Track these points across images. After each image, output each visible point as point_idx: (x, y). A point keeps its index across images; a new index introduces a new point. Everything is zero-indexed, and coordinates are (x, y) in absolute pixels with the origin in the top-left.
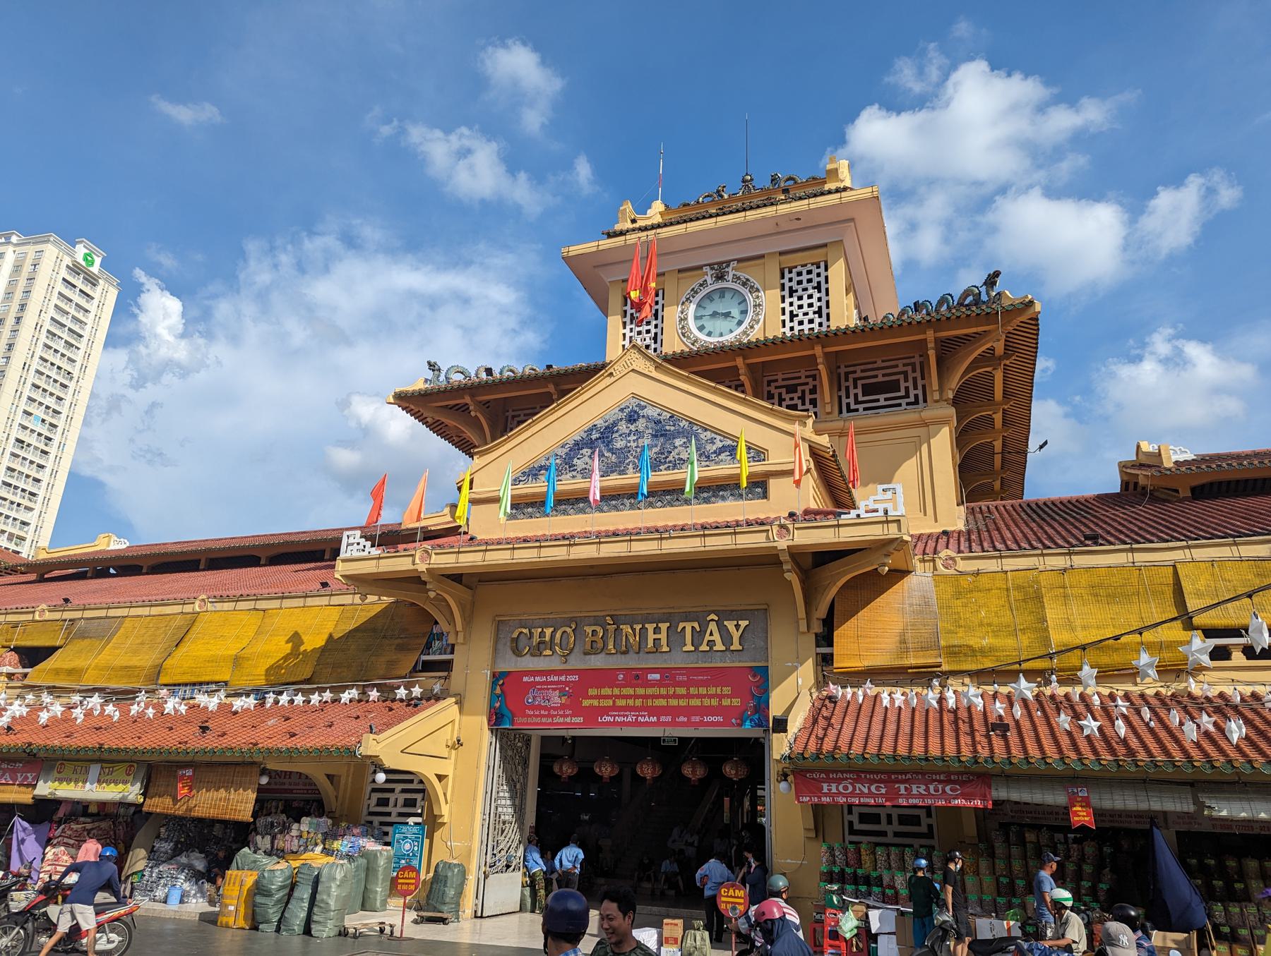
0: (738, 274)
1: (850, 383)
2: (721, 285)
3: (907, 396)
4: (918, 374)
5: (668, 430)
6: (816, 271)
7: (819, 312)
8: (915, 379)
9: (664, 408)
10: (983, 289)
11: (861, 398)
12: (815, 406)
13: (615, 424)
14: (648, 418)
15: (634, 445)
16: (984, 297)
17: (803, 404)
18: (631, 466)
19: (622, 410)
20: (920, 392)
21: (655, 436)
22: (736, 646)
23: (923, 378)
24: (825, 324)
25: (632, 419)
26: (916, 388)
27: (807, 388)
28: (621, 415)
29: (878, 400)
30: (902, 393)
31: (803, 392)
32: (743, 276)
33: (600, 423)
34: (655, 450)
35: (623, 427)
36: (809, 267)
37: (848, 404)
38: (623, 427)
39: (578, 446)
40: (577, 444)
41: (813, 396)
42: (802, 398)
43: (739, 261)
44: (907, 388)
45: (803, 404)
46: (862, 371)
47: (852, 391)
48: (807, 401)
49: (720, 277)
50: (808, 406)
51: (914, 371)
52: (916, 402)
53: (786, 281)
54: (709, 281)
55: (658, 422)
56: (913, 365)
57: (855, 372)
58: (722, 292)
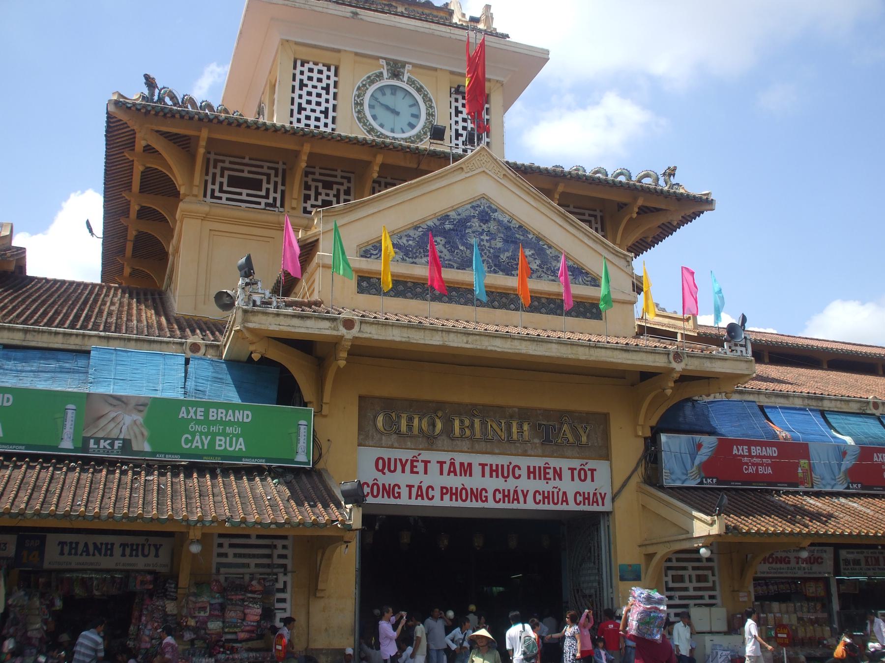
0: (414, 78)
5: (515, 235)
9: (512, 217)
13: (468, 219)
14: (500, 223)
15: (487, 244)
16: (661, 182)
19: (473, 207)
21: (506, 241)
24: (331, 126)
28: (472, 212)
33: (453, 214)
34: (507, 254)
38: (475, 223)
39: (432, 231)
40: (430, 229)
43: (415, 66)
49: (396, 75)
54: (385, 75)
55: (508, 228)
58: (394, 89)
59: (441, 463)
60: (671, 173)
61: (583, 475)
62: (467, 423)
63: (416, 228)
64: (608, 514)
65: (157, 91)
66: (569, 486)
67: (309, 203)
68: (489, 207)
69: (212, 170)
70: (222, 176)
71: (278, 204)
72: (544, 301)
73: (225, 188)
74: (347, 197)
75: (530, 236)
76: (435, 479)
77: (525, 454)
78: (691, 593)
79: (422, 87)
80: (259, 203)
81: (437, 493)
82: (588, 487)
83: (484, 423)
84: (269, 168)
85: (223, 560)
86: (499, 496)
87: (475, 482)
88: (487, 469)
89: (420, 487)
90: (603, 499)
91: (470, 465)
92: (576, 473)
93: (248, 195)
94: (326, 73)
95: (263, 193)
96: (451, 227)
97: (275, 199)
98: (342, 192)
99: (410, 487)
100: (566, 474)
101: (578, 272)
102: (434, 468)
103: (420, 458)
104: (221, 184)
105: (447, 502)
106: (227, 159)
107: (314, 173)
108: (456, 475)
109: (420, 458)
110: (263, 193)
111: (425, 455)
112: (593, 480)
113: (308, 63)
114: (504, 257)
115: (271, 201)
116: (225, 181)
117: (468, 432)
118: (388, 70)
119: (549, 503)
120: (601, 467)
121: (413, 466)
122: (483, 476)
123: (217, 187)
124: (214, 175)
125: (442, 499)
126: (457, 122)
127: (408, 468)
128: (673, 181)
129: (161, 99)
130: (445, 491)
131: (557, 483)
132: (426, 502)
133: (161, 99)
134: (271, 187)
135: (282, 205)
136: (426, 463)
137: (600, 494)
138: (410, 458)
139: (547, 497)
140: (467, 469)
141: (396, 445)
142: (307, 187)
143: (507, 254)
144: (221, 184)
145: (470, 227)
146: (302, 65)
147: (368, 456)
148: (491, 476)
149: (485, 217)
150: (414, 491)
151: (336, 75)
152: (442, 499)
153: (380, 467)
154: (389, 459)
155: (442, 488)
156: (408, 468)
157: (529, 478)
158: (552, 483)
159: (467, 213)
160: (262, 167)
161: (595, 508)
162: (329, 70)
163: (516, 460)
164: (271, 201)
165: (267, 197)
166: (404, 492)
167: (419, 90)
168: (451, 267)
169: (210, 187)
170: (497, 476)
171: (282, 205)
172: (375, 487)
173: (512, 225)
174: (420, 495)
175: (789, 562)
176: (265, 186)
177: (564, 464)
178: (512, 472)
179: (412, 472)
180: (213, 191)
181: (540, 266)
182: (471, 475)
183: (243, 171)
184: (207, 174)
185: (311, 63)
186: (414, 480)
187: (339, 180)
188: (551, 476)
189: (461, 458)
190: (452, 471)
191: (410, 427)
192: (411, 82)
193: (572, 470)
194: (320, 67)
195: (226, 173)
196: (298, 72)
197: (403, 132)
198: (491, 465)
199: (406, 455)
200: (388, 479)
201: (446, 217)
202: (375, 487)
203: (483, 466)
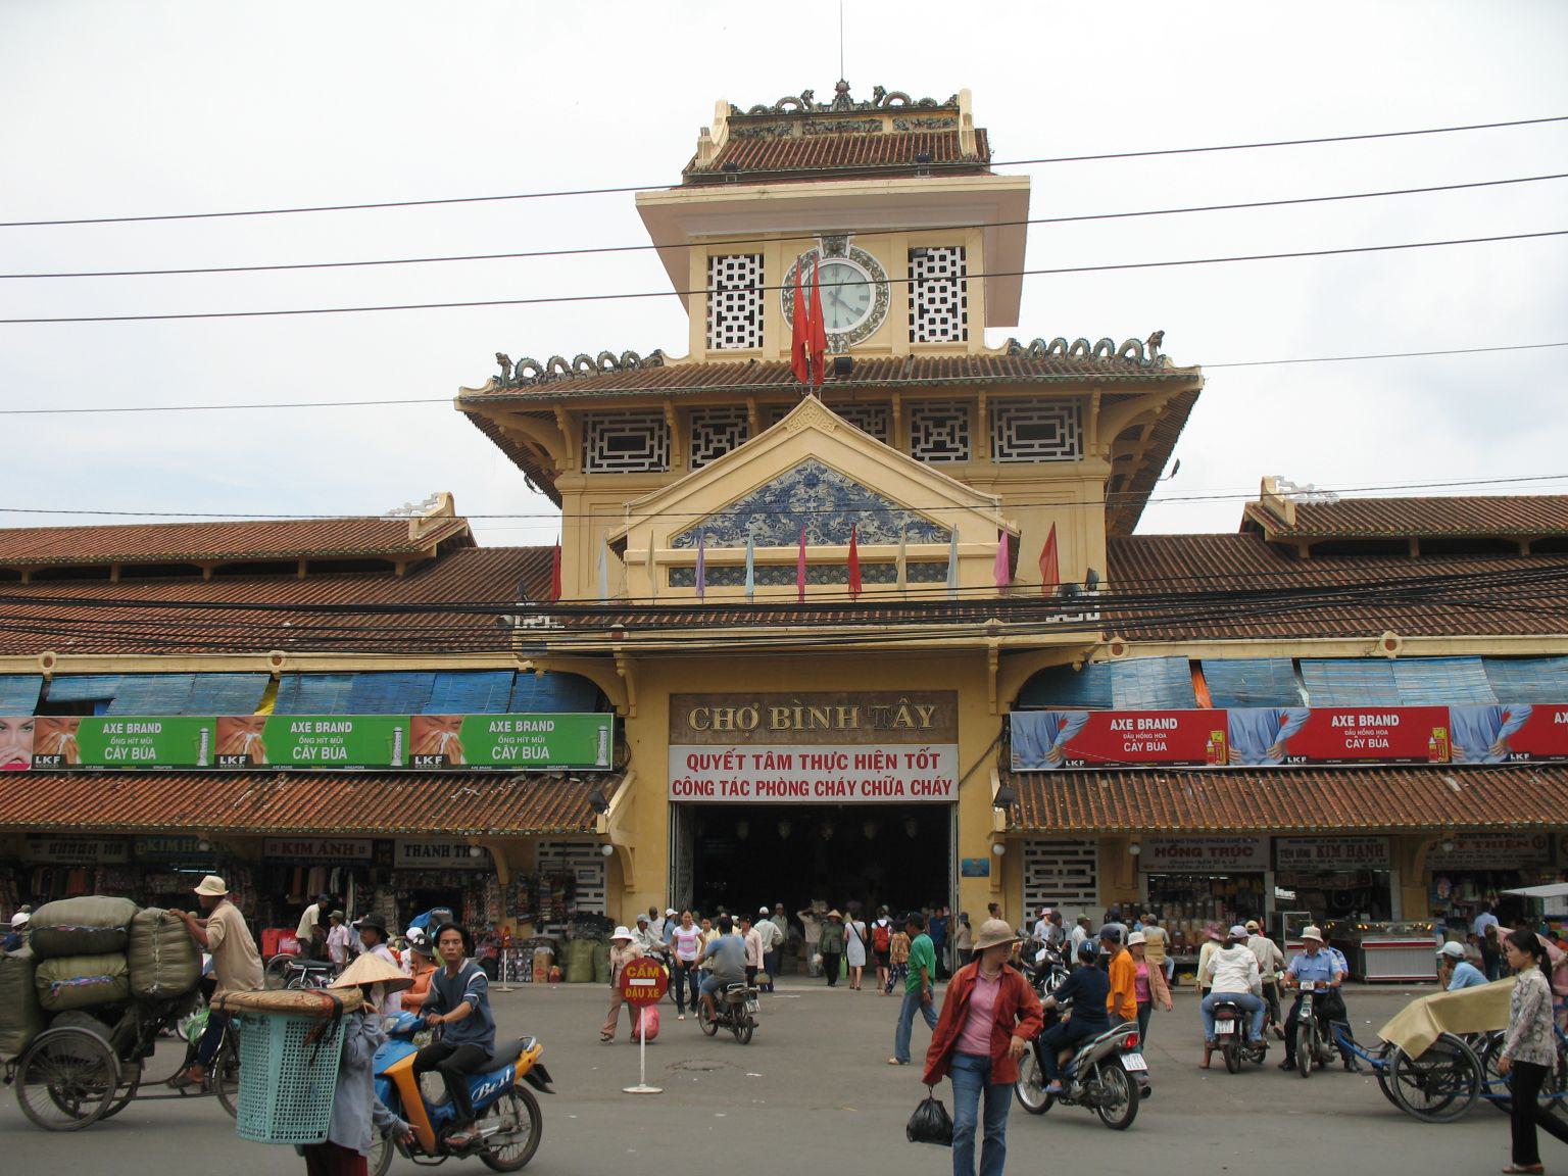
1: (1004, 424)
2: (835, 260)
3: (1062, 444)
4: (1074, 421)
6: (950, 258)
7: (953, 310)
8: (1071, 426)
10: (1146, 348)
11: (1014, 442)
12: (965, 446)
13: (792, 487)
14: (830, 485)
17: (953, 441)
18: (811, 537)
19: (799, 471)
20: (1075, 441)
22: (926, 724)
23: (1079, 426)
25: (812, 482)
26: (1071, 436)
27: (957, 423)
28: (798, 478)
29: (1032, 446)
30: (1058, 440)
31: (953, 427)
32: (866, 250)
33: (774, 484)
35: (801, 491)
36: (943, 252)
37: (1001, 447)
38: (801, 491)
40: (748, 504)
41: (963, 434)
42: (951, 435)
44: (1063, 436)
45: (953, 441)
46: (1017, 410)
47: (1006, 433)
48: (957, 439)
50: (957, 445)
51: (1070, 417)
52: (1071, 453)
53: (914, 265)
54: (821, 254)
55: (840, 489)
56: (1070, 410)
57: (1009, 410)
59: (757, 757)
60: (1156, 340)
61: (922, 762)
62: (787, 712)
63: (733, 506)
64: (957, 802)
65: (513, 369)
66: (905, 774)
67: (699, 454)
68: (818, 468)
69: (590, 435)
70: (602, 440)
71: (664, 463)
72: (883, 568)
73: (606, 453)
74: (741, 440)
75: (867, 495)
76: (751, 774)
77: (854, 742)
78: (1060, 890)
79: (870, 259)
80: (643, 465)
81: (752, 789)
82: (929, 775)
83: (805, 714)
84: (652, 421)
85: (544, 858)
86: (821, 788)
87: (795, 774)
88: (809, 761)
89: (734, 783)
90: (947, 788)
91: (789, 757)
92: (914, 760)
93: (630, 457)
94: (749, 266)
95: (647, 452)
96: (773, 498)
97: (660, 456)
98: (736, 435)
99: (724, 783)
100: (902, 762)
101: (927, 528)
102: (749, 762)
103: (734, 753)
104: (601, 449)
105: (764, 797)
106: (606, 419)
107: (703, 418)
108: (773, 768)
109: (734, 753)
110: (647, 452)
111: (741, 750)
112: (935, 767)
113: (726, 258)
114: (834, 524)
115: (655, 459)
116: (605, 445)
117: (787, 723)
118: (824, 246)
119: (880, 794)
120: (946, 752)
121: (726, 762)
122: (804, 767)
123: (596, 454)
124: (593, 441)
125: (758, 794)
126: (921, 295)
127: (721, 764)
128: (1159, 351)
129: (519, 375)
130: (760, 785)
131: (891, 771)
132: (741, 798)
133: (519, 375)
134: (656, 443)
135: (667, 464)
136: (741, 757)
137: (944, 781)
138: (723, 753)
139: (877, 787)
140: (785, 762)
141: (710, 741)
142: (697, 436)
143: (838, 520)
144: (601, 449)
145: (795, 496)
146: (720, 263)
147: (682, 752)
148: (813, 768)
149: (812, 482)
150: (728, 787)
151: (761, 266)
152: (758, 794)
153: (693, 764)
154: (702, 756)
155: (758, 783)
156: (721, 764)
157: (857, 767)
158: (884, 772)
159: (791, 480)
160: (644, 421)
161: (936, 798)
162: (752, 261)
163: (841, 749)
164: (655, 459)
165: (651, 456)
166: (718, 788)
167: (866, 263)
168: (771, 544)
169: (589, 454)
170: (820, 768)
171: (667, 464)
172: (688, 785)
173: (844, 485)
174: (734, 790)
175: (1200, 854)
176: (648, 443)
177: (899, 750)
178: (838, 762)
179: (726, 767)
180: (593, 458)
181: (879, 528)
182: (790, 768)
183: (623, 430)
184: (585, 440)
185: (730, 258)
186: (729, 776)
187: (732, 420)
188: (884, 764)
189: (779, 750)
190: (770, 764)
191: (723, 723)
192: (855, 255)
193: (910, 757)
194: (742, 260)
195: (606, 436)
196: (714, 273)
197: (850, 323)
198: (813, 757)
199: (719, 750)
200: (700, 776)
201: (766, 489)
202: (688, 785)
203: (804, 757)
